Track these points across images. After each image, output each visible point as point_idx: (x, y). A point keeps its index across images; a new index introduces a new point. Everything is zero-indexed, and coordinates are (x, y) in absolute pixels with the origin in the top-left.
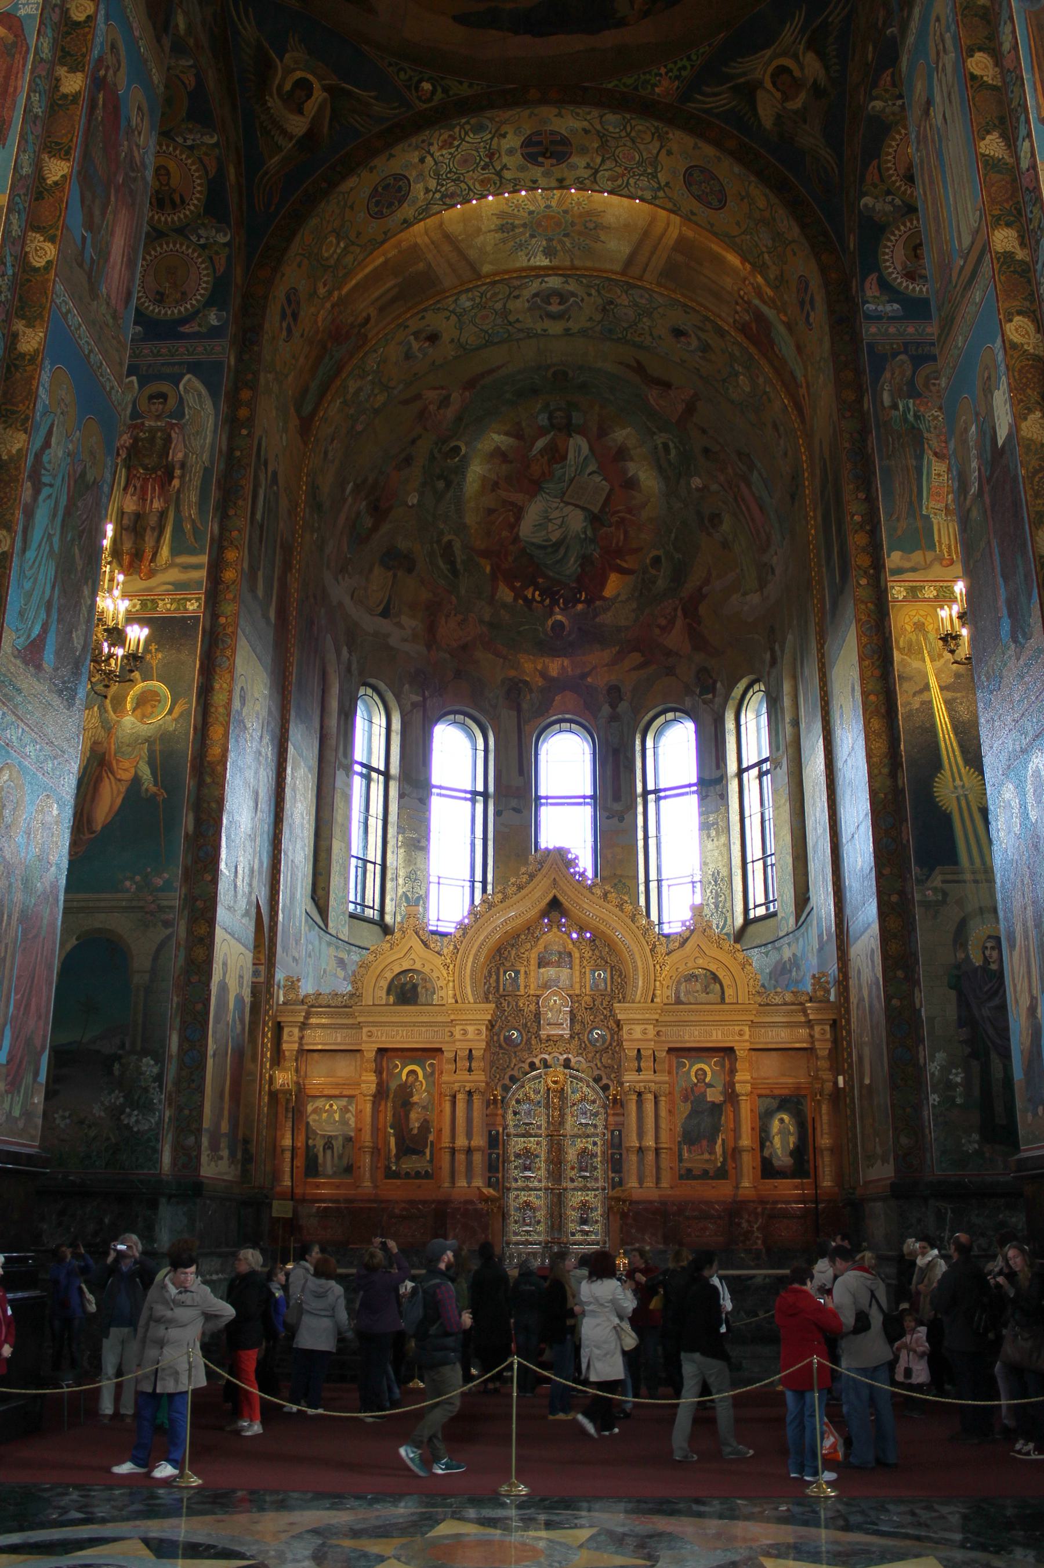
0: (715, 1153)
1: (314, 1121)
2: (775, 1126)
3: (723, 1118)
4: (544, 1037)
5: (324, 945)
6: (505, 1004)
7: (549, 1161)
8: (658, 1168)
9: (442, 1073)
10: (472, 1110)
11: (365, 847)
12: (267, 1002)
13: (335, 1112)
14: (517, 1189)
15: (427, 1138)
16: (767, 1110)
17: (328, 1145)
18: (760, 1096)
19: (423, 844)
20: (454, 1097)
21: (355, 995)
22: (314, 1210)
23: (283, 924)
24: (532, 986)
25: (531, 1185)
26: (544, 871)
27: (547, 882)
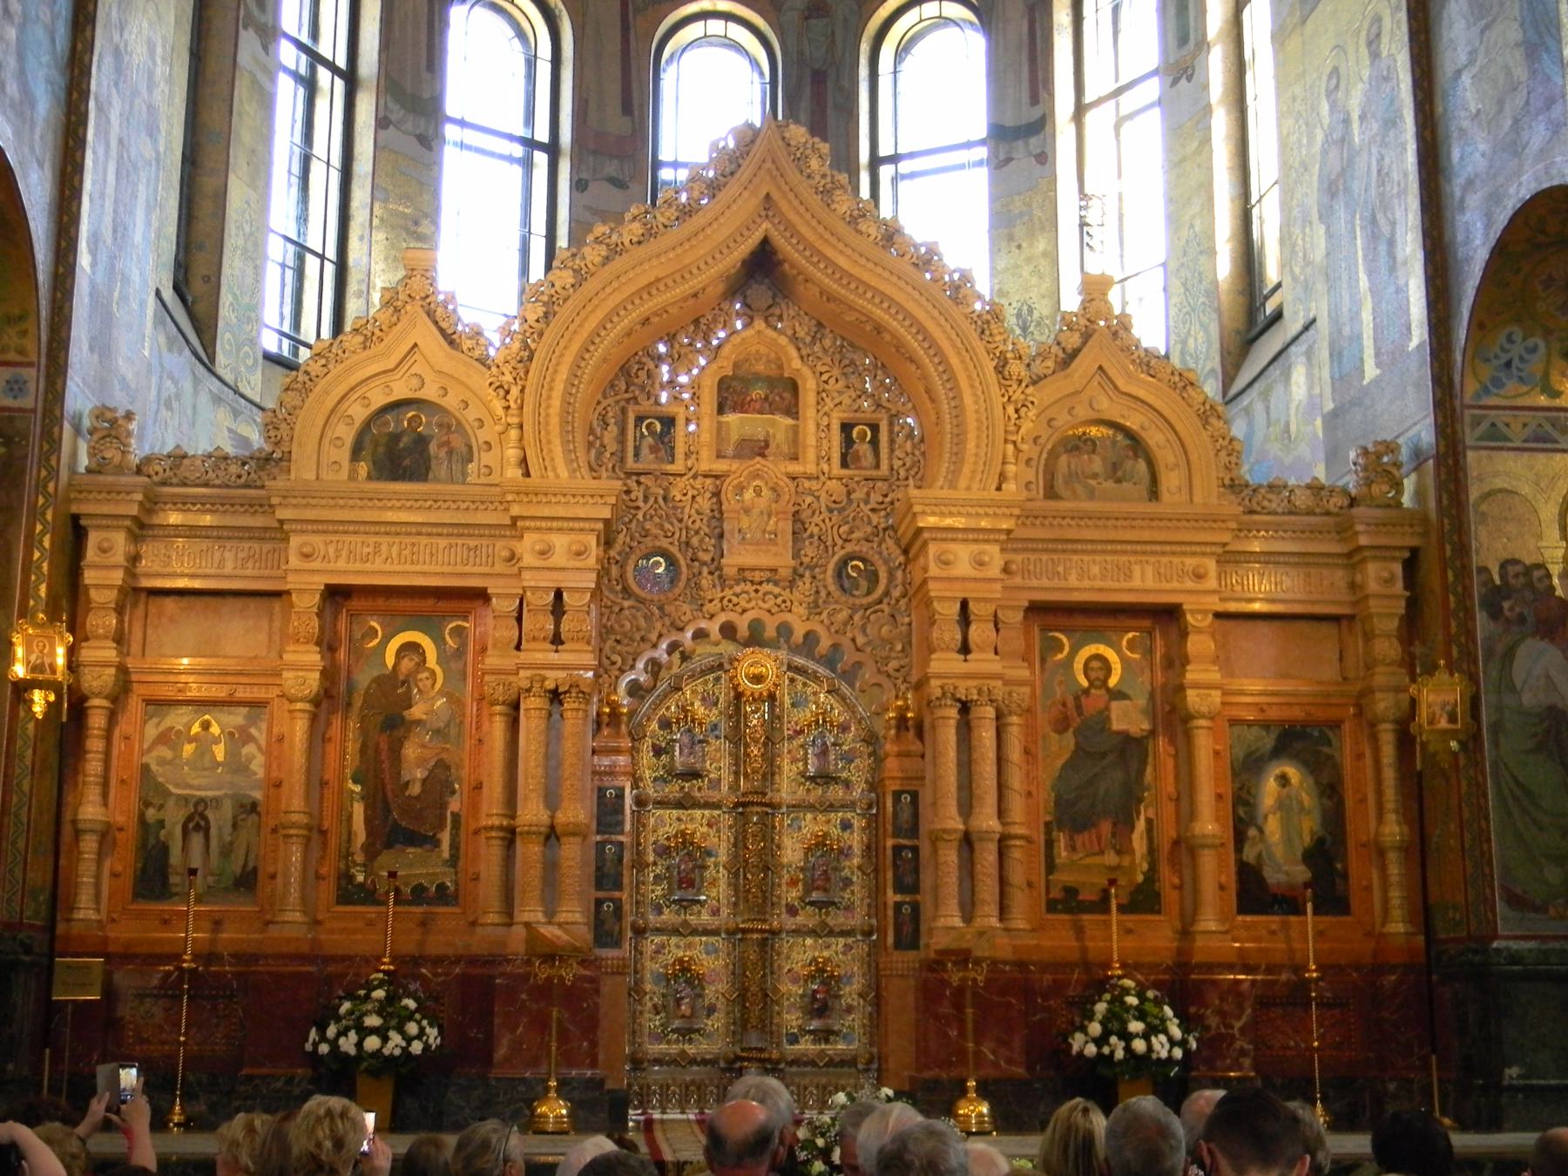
0: (1132, 852)
1: (162, 762)
2: (1269, 790)
3: (1149, 770)
4: (730, 571)
5: (204, 399)
6: (638, 493)
7: (737, 868)
8: (1003, 881)
9: (484, 650)
10: (559, 738)
11: (303, 218)
12: (45, 459)
13: (216, 741)
14: (659, 931)
15: (444, 806)
16: (1248, 756)
17: (197, 822)
18: (1234, 722)
19: (425, 228)
20: (516, 706)
21: (266, 463)
22: (155, 982)
23: (93, 284)
24: (704, 453)
25: (692, 919)
26: (744, 174)
27: (752, 202)
